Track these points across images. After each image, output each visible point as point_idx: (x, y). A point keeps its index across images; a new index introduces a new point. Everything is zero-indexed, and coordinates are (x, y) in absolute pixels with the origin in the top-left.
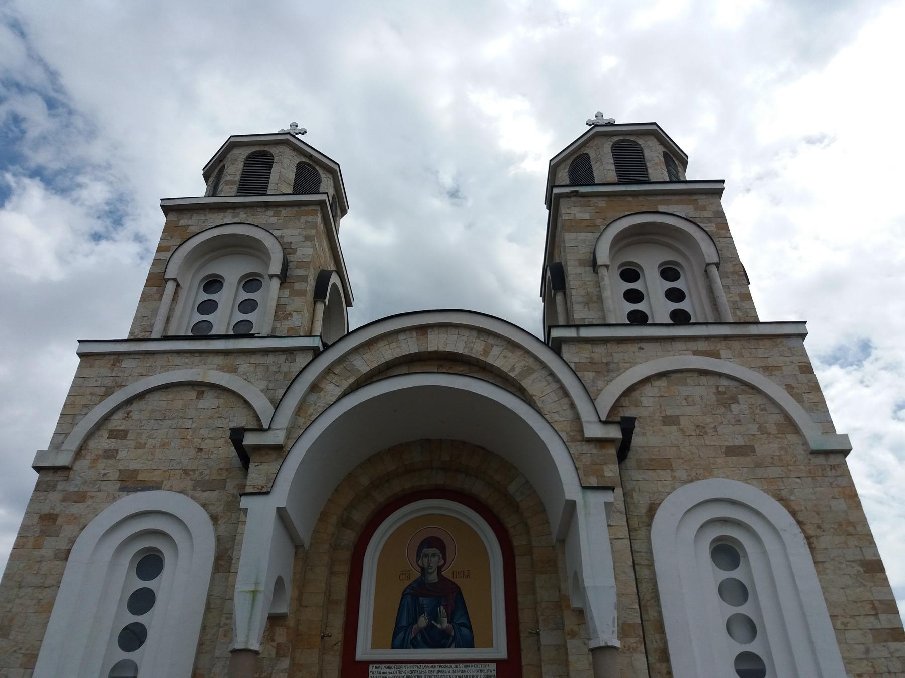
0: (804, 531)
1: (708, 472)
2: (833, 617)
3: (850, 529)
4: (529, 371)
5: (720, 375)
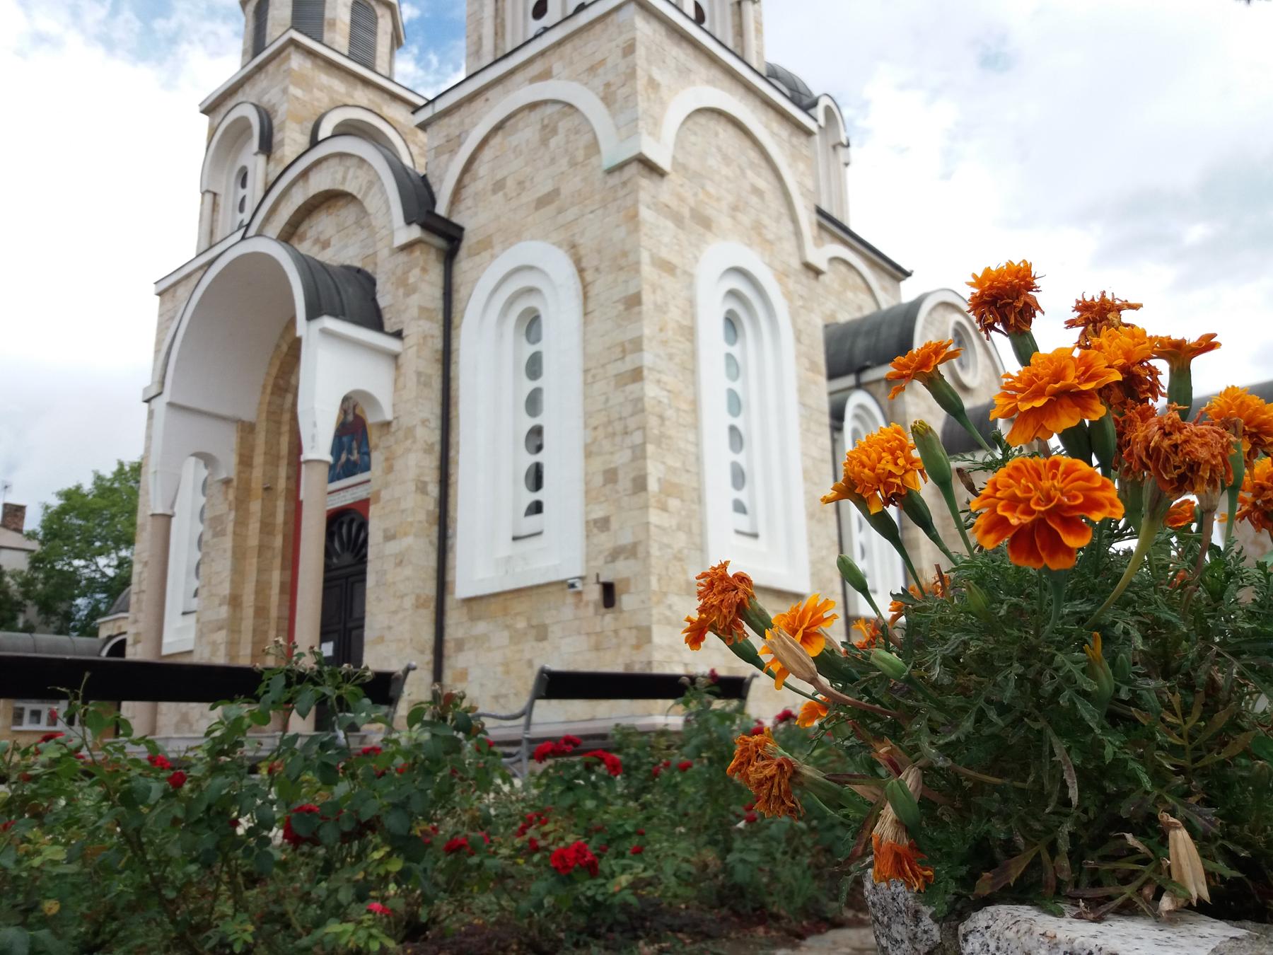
0: (582, 279)
1: (519, 237)
2: (586, 371)
4: (371, 184)
5: (545, 102)
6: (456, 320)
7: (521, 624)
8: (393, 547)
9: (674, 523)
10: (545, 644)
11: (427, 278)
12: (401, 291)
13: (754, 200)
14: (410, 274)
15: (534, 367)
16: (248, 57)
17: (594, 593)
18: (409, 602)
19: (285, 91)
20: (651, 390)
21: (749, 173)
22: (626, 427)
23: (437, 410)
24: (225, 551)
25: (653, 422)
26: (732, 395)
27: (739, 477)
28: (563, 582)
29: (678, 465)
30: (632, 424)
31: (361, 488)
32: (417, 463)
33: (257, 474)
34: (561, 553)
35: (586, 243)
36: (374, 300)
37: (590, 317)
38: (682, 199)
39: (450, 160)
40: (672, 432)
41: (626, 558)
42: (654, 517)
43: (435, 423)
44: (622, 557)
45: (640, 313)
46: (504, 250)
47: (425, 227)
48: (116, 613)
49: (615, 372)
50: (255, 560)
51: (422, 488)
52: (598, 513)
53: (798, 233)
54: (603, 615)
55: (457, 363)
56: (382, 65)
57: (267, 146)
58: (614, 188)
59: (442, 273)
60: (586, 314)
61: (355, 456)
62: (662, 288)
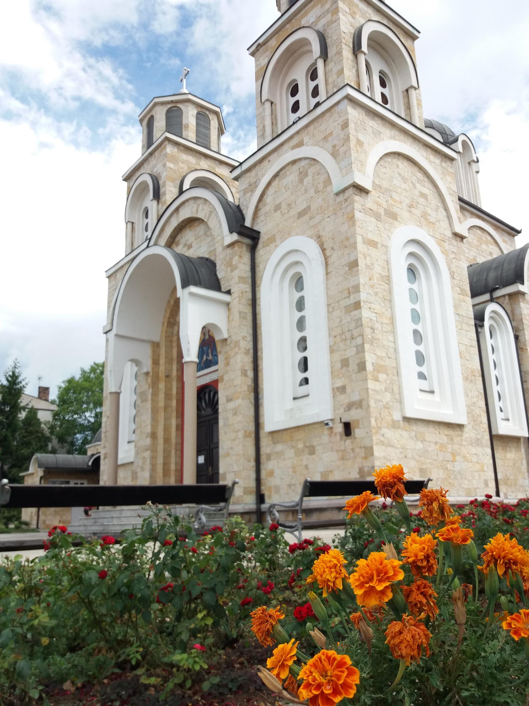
1: (289, 235)
2: (328, 305)
3: (347, 244)
5: (300, 159)
6: (258, 282)
7: (300, 445)
8: (231, 405)
9: (383, 387)
10: (314, 456)
11: (242, 261)
12: (229, 269)
13: (422, 200)
14: (234, 260)
15: (300, 305)
16: (145, 149)
17: (339, 428)
18: (241, 434)
19: (164, 165)
20: (365, 314)
21: (418, 185)
22: (352, 335)
23: (251, 331)
24: (148, 409)
25: (368, 331)
26: (414, 311)
27: (420, 359)
28: (322, 422)
29: (384, 354)
30: (356, 333)
31: (214, 374)
32: (241, 360)
33: (162, 368)
34: (320, 406)
35: (326, 235)
36: (216, 274)
37: (329, 276)
38: (379, 205)
39: (251, 196)
40: (379, 336)
41: (356, 409)
42: (371, 385)
43: (250, 338)
44: (354, 408)
45: (358, 271)
46: (282, 242)
47: (240, 233)
48: (95, 442)
49: (345, 305)
50: (163, 414)
51: (244, 373)
52: (339, 383)
53: (449, 217)
54: (345, 441)
55: (259, 305)
56: (214, 146)
57: (157, 195)
58: (340, 203)
59: (250, 257)
60: (327, 274)
61: (210, 357)
62: (370, 256)
